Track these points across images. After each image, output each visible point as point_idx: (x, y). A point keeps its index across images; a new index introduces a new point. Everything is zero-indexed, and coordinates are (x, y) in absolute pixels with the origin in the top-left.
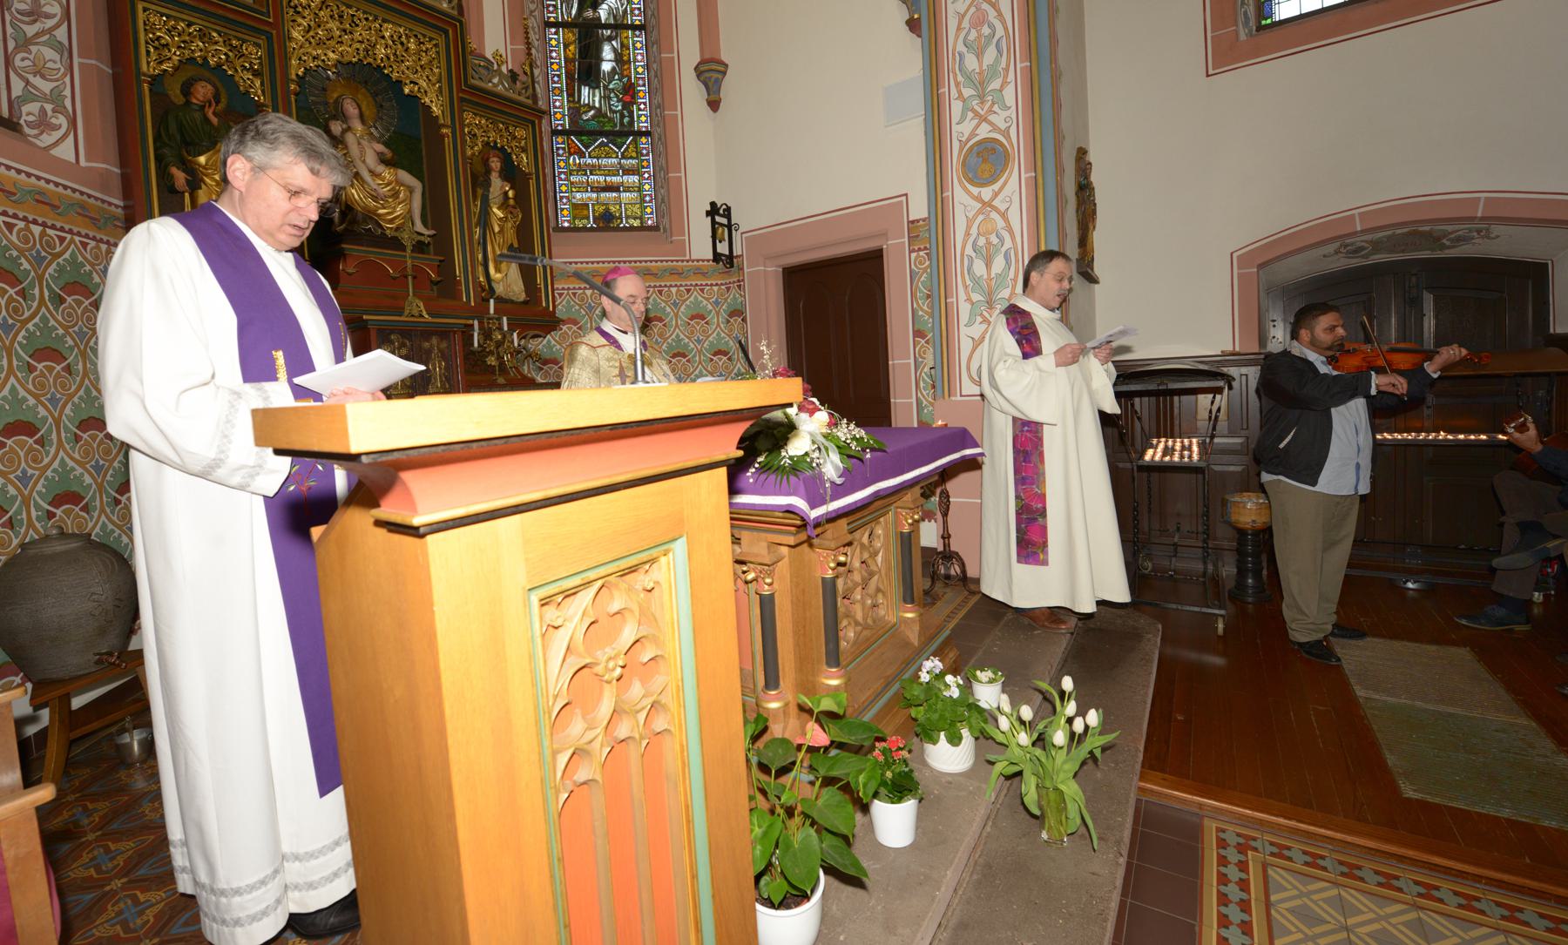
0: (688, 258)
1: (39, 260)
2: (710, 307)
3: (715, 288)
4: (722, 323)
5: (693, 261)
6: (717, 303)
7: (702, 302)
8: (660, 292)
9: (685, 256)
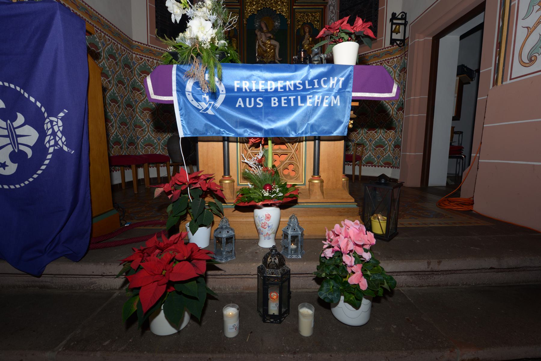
0: (383, 47)
2: (391, 70)
4: (397, 77)
5: (385, 48)
6: (395, 67)
7: (388, 68)
9: (382, 47)
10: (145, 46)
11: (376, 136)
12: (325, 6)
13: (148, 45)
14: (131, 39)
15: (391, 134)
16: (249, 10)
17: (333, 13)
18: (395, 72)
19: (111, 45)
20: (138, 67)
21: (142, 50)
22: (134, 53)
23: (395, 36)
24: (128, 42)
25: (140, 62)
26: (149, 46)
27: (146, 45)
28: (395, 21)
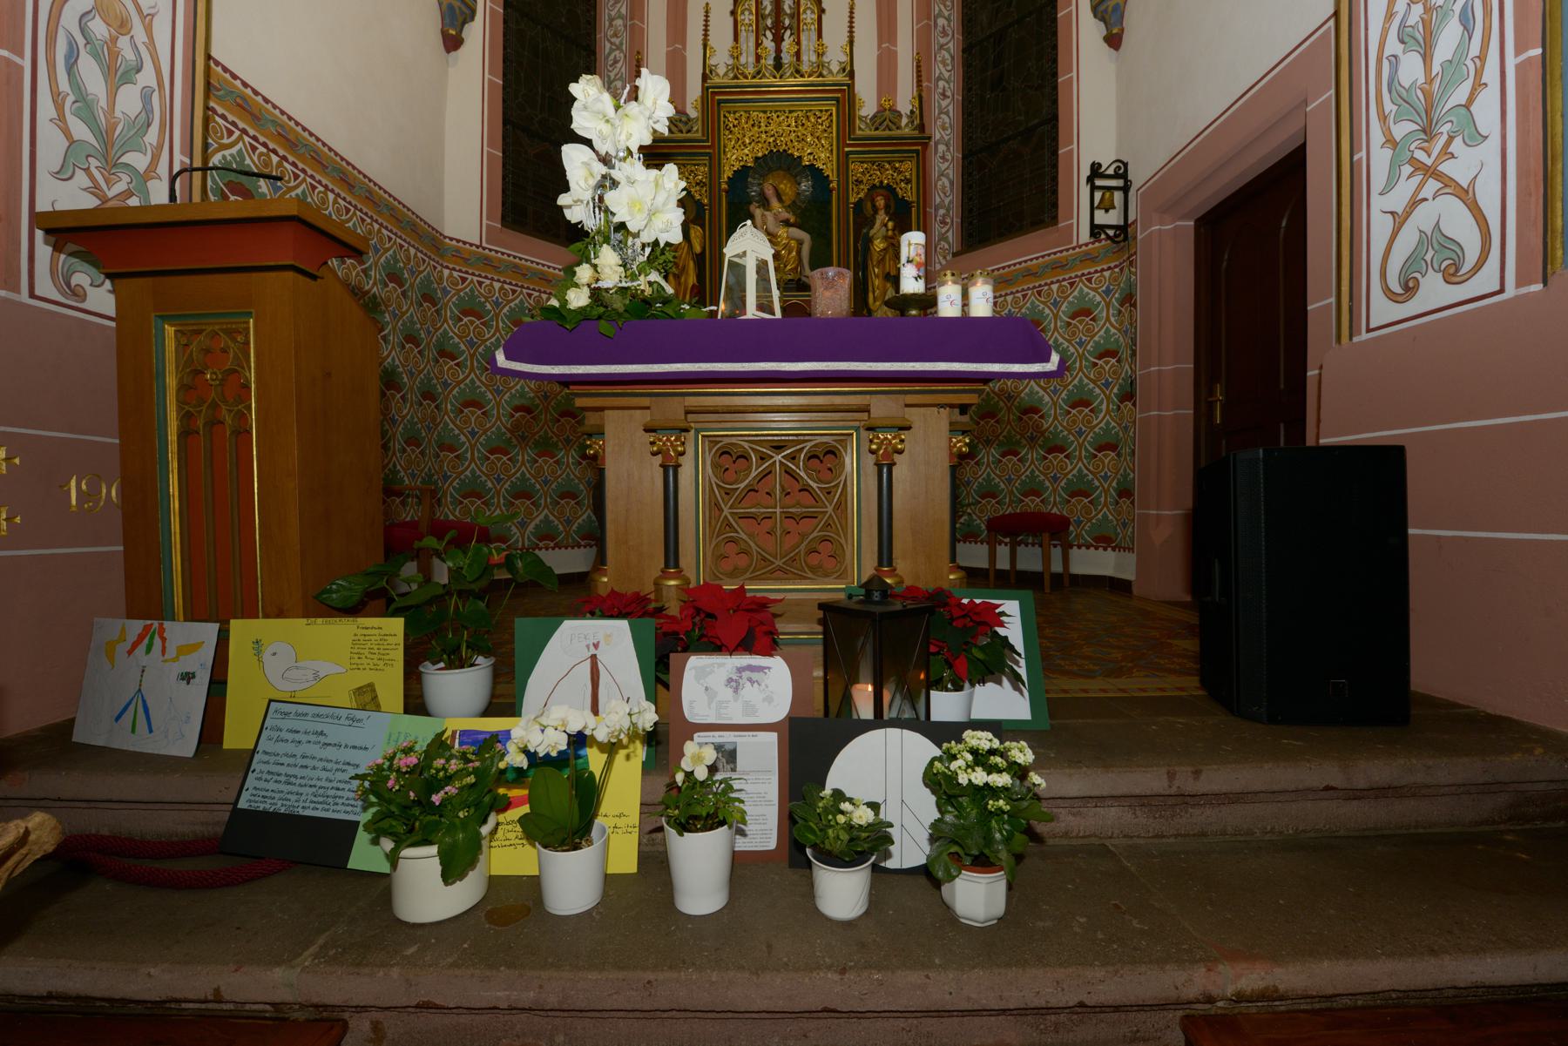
0: (1075, 244)
1: (497, 304)
2: (1098, 298)
3: (1107, 274)
4: (1113, 315)
5: (1080, 247)
6: (1107, 292)
7: (1088, 294)
8: (1039, 293)
9: (1072, 243)
10: (474, 248)
11: (1069, 468)
12: (925, 146)
13: (481, 246)
14: (441, 234)
15: (1106, 461)
16: (734, 157)
17: (947, 160)
18: (1108, 305)
19: (395, 252)
20: (454, 299)
21: (466, 260)
22: (447, 267)
23: (1101, 218)
24: (432, 241)
25: (460, 287)
26: (484, 249)
27: (477, 247)
28: (1098, 182)
